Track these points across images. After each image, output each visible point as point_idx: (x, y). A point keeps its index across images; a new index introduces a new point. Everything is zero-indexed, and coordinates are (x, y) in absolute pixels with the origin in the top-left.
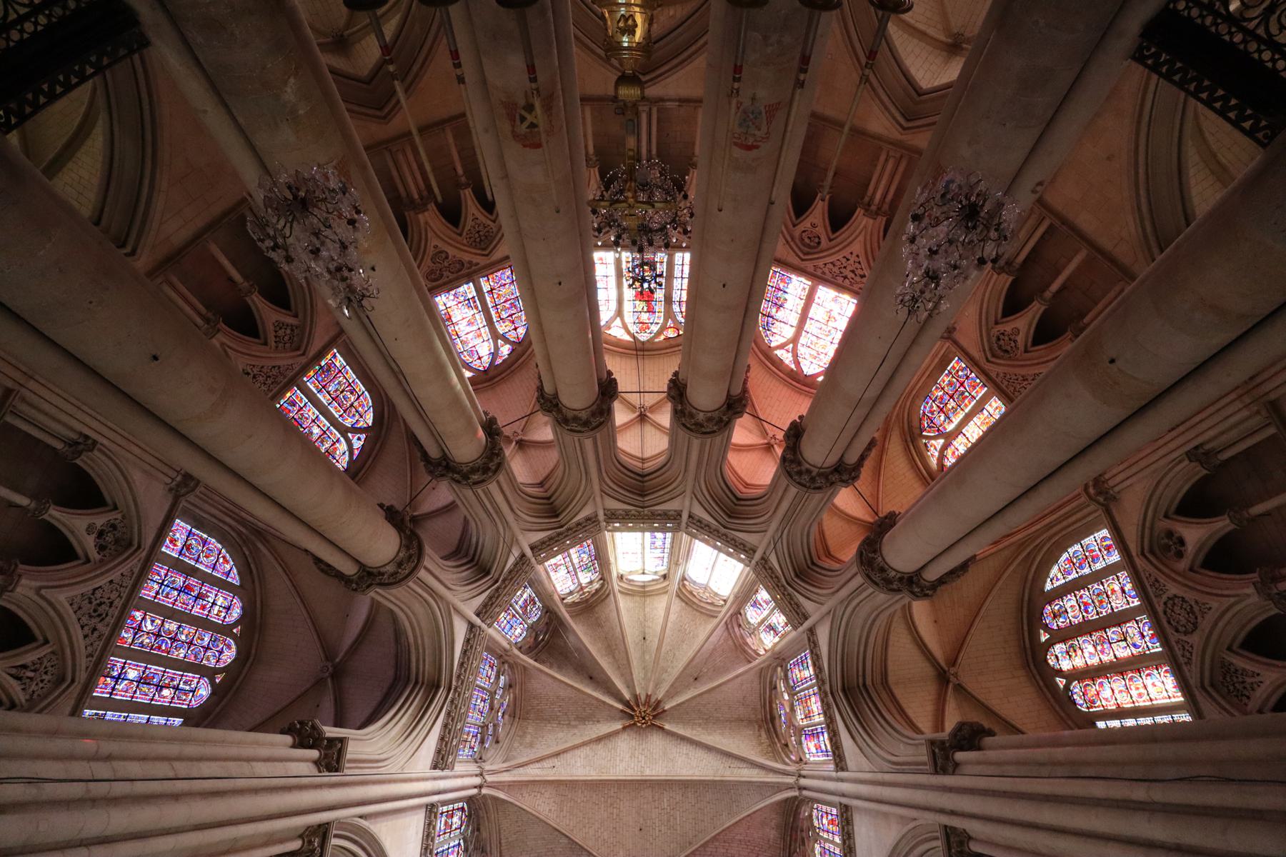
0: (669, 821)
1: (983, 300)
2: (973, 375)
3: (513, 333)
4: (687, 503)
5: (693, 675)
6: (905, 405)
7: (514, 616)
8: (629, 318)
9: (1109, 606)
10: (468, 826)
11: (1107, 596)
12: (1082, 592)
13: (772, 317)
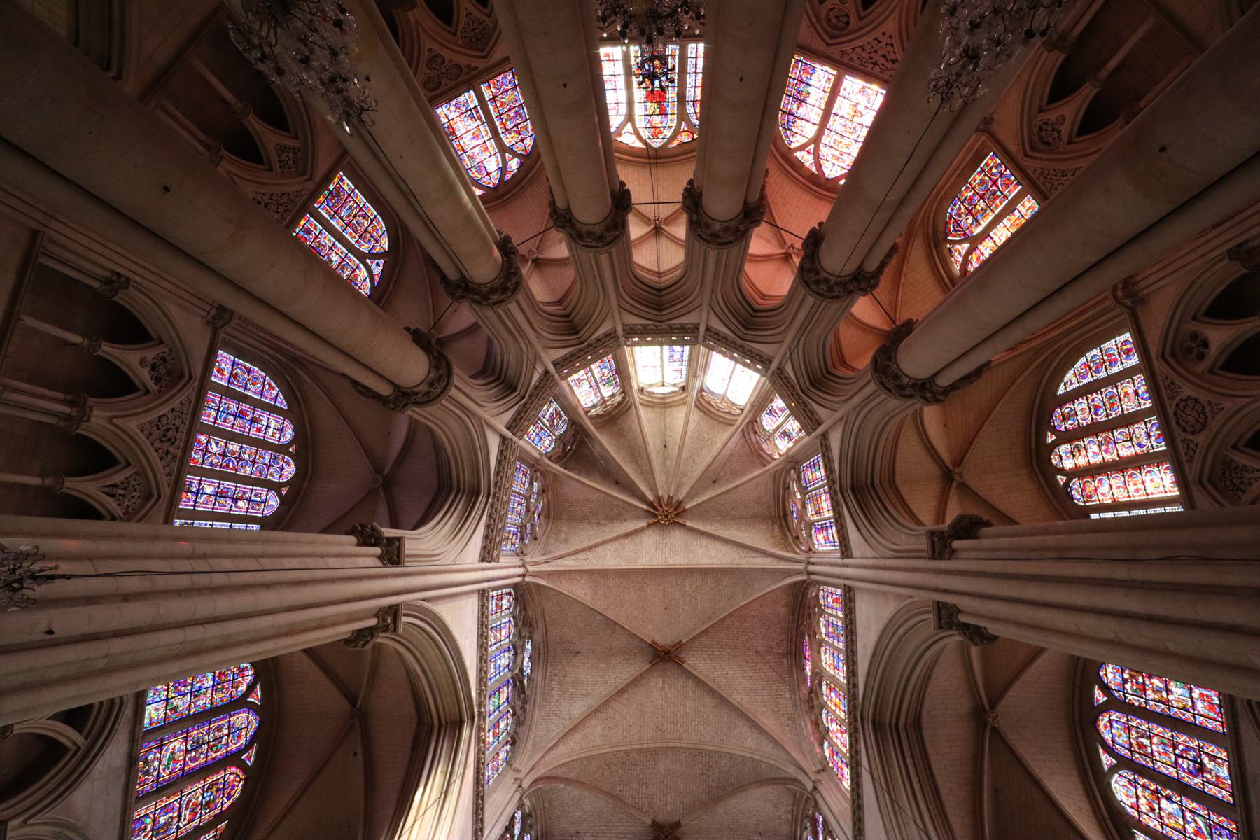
0: (691, 601)
1: (1028, 83)
2: (1008, 171)
3: (520, 145)
4: (704, 316)
5: (712, 477)
6: (931, 209)
7: (542, 429)
8: (640, 122)
9: (1120, 408)
10: (515, 607)
11: (1120, 399)
12: (1095, 395)
13: (793, 114)
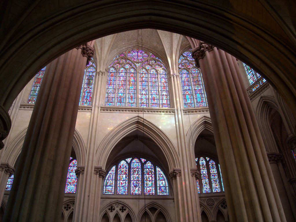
12: (217, 176)
